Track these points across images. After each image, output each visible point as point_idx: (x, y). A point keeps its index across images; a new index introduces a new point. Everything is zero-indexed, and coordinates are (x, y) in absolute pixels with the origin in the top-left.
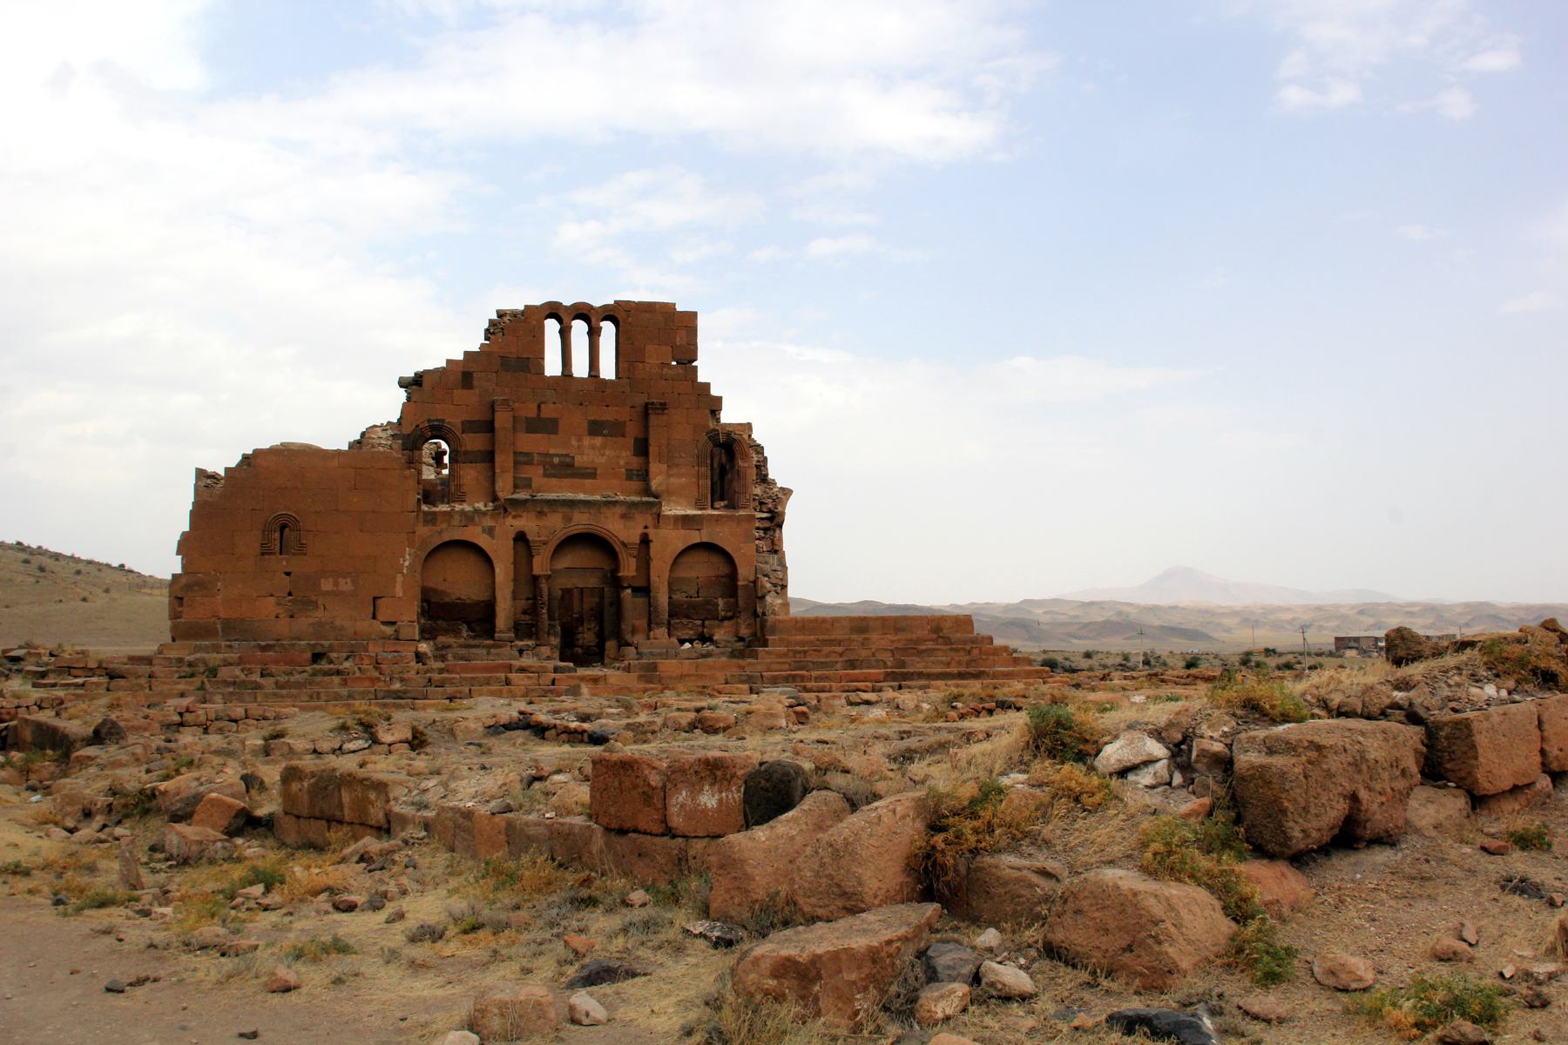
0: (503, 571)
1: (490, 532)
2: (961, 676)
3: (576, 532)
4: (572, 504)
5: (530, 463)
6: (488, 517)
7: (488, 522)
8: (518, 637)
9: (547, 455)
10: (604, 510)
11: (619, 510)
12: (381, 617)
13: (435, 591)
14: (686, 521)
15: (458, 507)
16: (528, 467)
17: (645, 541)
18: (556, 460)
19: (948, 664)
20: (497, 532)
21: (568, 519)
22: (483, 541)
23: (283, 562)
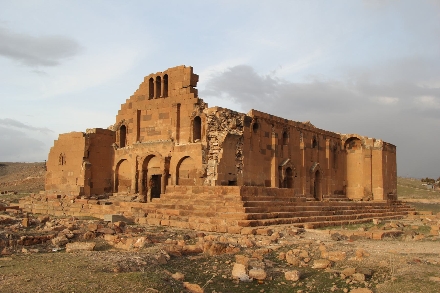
1: (131, 156)
2: (208, 215)
3: (149, 155)
4: (149, 144)
6: (130, 151)
7: (130, 152)
11: (162, 145)
13: (121, 176)
14: (182, 148)
16: (143, 132)
18: (150, 129)
20: (133, 155)
21: (149, 150)
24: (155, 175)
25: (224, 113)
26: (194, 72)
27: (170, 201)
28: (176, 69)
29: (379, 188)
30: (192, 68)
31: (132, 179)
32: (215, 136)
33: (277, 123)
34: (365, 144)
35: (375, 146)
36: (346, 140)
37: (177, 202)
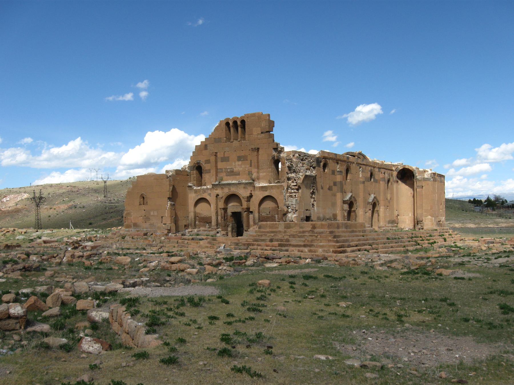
0: (213, 206)
1: (210, 195)
2: (305, 246)
5: (222, 172)
8: (217, 228)
9: (225, 169)
10: (238, 186)
11: (243, 186)
12: (163, 223)
13: (199, 214)
15: (203, 187)
17: (251, 196)
18: (229, 170)
19: (304, 241)
21: (230, 189)
22: (208, 198)
23: (143, 207)
24: (235, 212)
25: (300, 155)
26: (271, 119)
27: (266, 235)
28: (253, 115)
29: (429, 217)
30: (269, 115)
31: (212, 216)
32: (293, 177)
33: (341, 161)
34: (417, 175)
35: (426, 176)
36: (398, 171)
37: (273, 237)
